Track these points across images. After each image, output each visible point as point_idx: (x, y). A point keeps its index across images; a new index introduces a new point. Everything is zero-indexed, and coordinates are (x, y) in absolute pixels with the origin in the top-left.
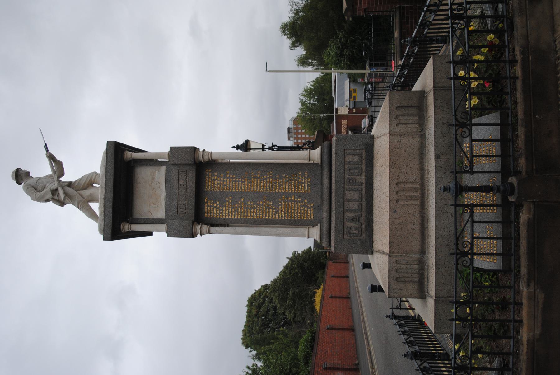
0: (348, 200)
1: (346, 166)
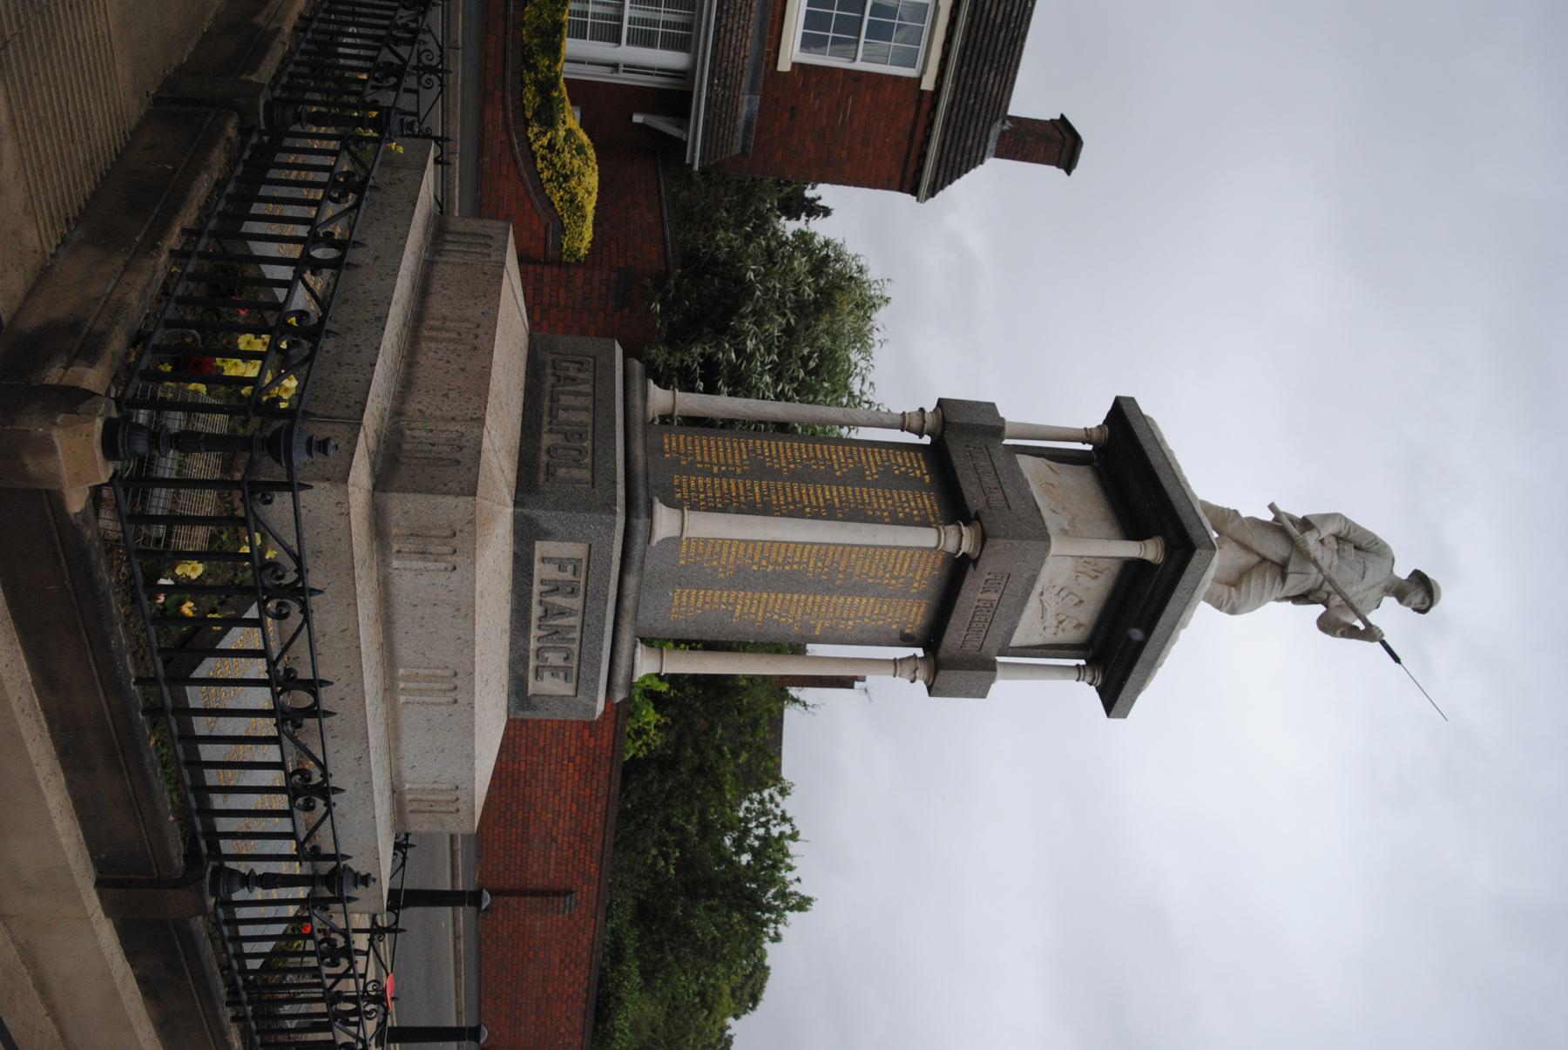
0: (586, 409)
1: (588, 460)
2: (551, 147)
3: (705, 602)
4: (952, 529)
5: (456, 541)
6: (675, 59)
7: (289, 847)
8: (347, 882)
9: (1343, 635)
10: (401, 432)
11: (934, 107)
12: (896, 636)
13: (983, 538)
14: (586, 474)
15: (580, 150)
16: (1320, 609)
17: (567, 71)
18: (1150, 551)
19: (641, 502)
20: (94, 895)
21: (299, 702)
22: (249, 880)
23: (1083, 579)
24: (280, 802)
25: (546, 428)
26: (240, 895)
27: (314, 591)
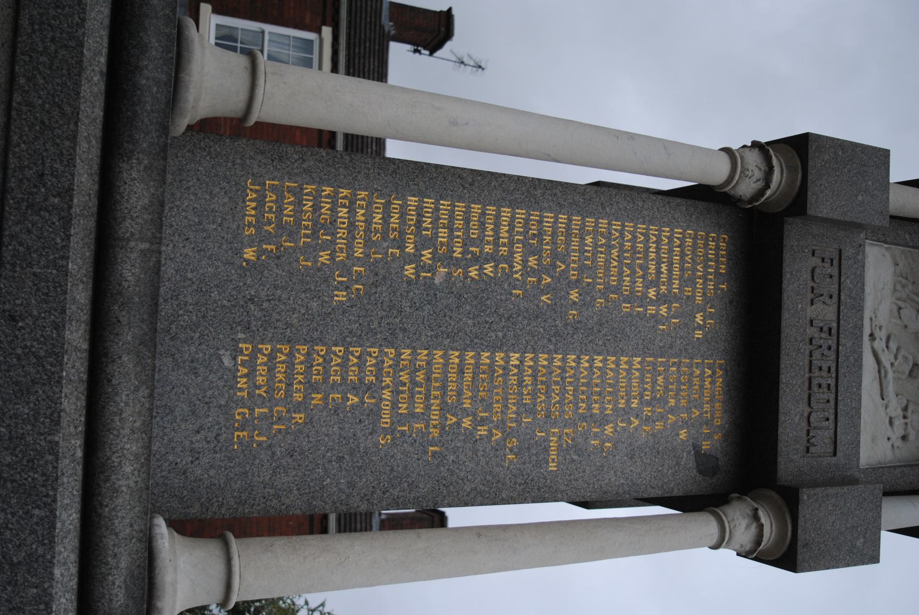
3: (312, 387)
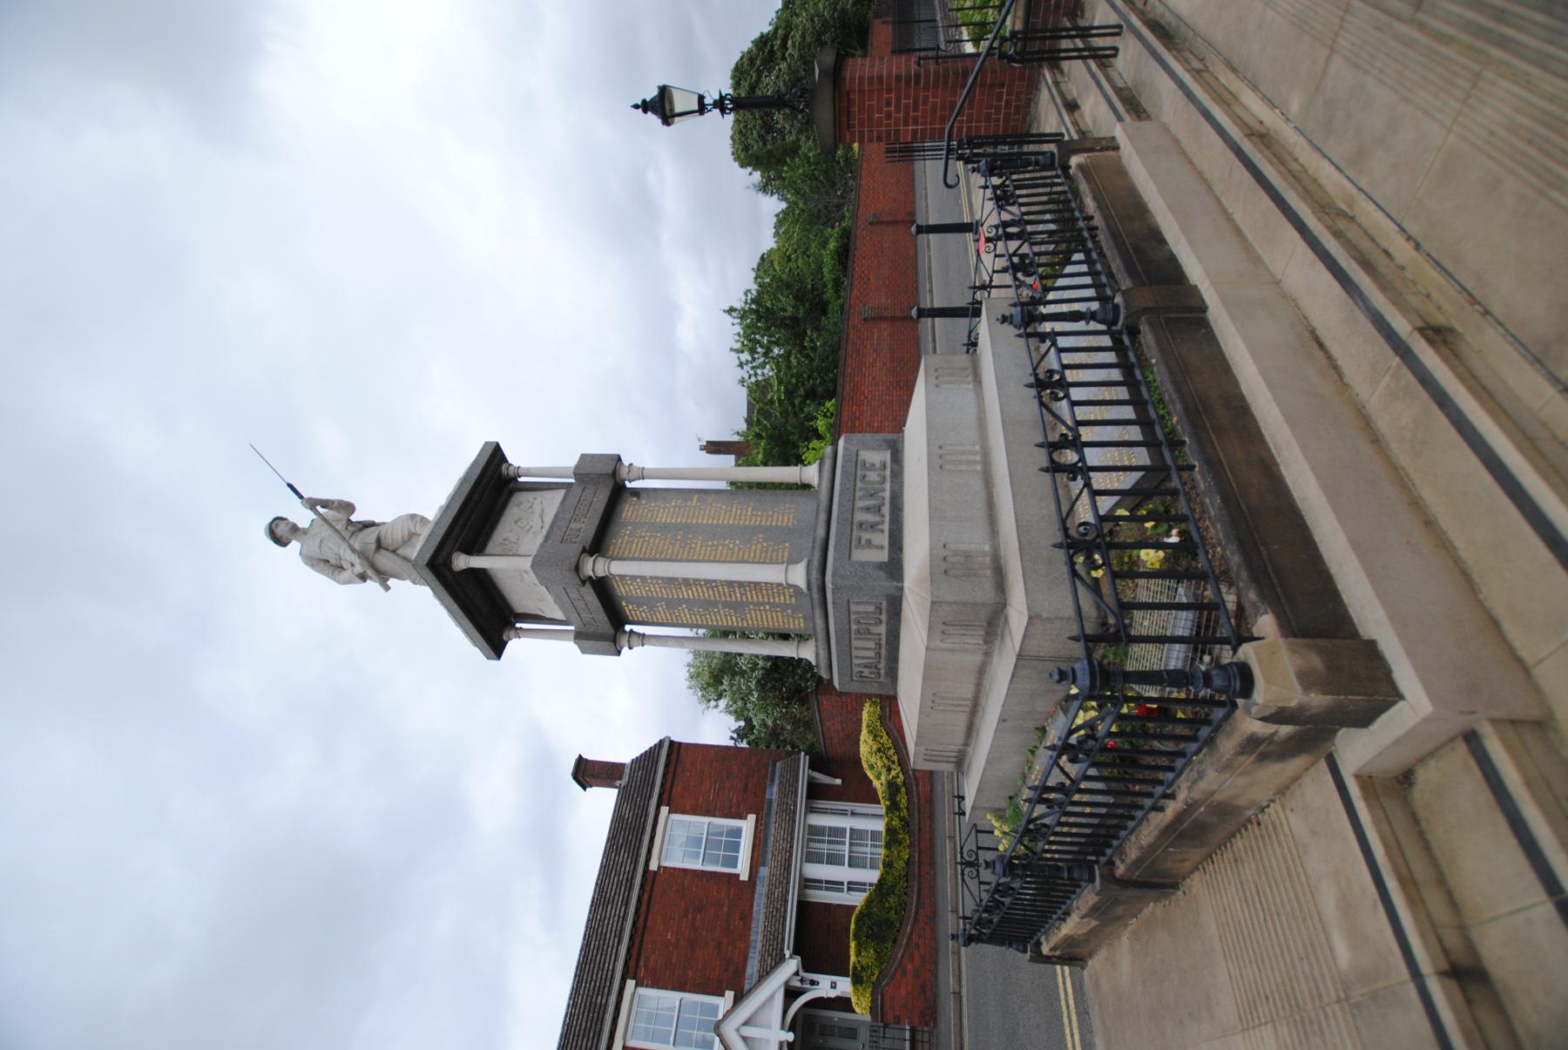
1: (853, 617)
2: (889, 770)
4: (600, 573)
5: (944, 566)
6: (817, 820)
7: (1063, 342)
8: (1018, 320)
9: (333, 502)
10: (986, 642)
11: (660, 795)
12: (643, 495)
13: (577, 569)
14: (854, 608)
15: (871, 767)
16: (354, 518)
17: (881, 809)
18: (462, 562)
19: (815, 590)
20: (1208, 301)
21: (1061, 456)
22: (1092, 316)
23: (513, 538)
24: (1071, 376)
25: (884, 638)
26: (1095, 306)
27: (1059, 546)
